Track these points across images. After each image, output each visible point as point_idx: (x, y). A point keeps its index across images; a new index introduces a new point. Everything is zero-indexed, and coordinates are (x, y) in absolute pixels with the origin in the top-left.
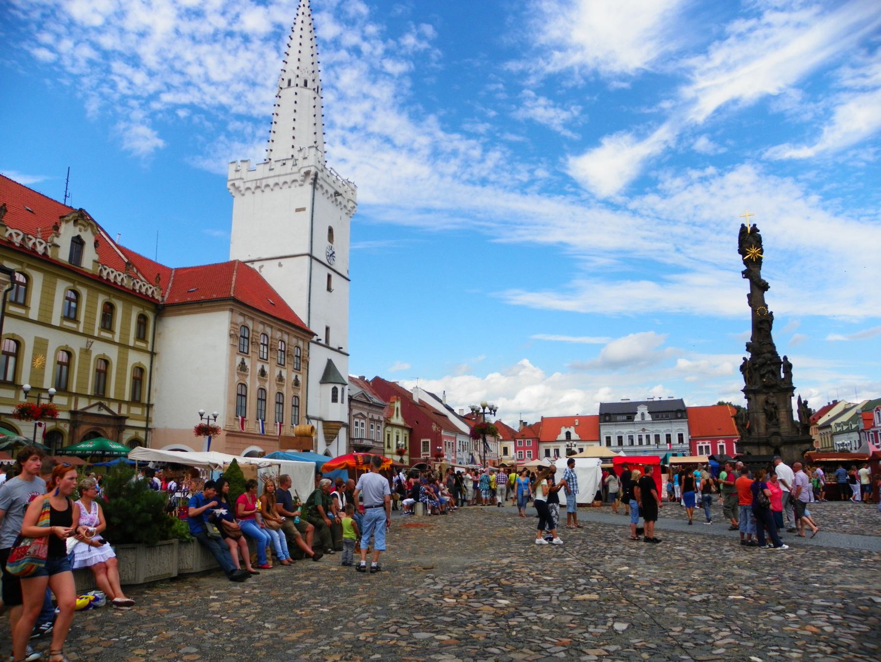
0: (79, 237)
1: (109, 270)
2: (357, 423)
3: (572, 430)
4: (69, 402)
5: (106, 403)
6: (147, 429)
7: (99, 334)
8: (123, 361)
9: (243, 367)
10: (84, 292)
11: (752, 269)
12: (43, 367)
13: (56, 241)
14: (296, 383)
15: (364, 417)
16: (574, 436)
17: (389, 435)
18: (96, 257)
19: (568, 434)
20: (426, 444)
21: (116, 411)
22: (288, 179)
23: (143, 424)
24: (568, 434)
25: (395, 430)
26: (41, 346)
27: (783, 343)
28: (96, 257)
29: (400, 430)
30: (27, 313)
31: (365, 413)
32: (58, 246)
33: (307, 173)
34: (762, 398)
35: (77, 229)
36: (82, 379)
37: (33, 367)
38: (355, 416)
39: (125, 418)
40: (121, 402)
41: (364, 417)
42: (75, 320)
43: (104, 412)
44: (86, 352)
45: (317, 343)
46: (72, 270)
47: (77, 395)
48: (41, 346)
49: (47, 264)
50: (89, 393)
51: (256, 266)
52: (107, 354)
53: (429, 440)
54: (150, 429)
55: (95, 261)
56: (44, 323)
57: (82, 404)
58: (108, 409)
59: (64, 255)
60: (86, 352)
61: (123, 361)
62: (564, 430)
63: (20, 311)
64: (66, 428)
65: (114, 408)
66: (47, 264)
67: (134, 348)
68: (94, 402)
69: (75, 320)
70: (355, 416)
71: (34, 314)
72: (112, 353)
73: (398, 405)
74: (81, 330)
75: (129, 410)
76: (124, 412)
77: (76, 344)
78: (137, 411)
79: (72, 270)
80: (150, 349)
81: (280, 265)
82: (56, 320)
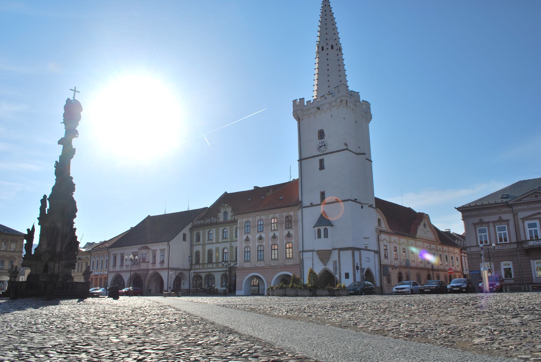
38: (524, 219)
56: (217, 242)
63: (211, 242)
69: (226, 238)
70: (524, 219)
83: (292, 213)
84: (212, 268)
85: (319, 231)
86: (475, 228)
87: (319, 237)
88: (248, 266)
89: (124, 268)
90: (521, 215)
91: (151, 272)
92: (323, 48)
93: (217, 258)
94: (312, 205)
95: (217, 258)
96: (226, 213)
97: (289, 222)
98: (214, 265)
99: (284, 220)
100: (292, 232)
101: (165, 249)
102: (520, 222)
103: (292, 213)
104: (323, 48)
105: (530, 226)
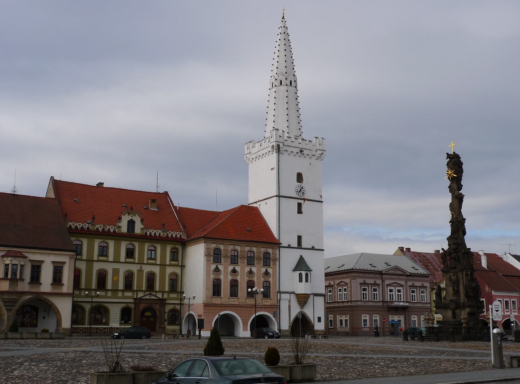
0: (132, 219)
1: (150, 231)
4: (133, 294)
5: (154, 293)
6: (181, 304)
7: (147, 261)
8: (163, 273)
9: (217, 270)
12: (118, 280)
13: (119, 224)
18: (142, 226)
21: (161, 297)
22: (267, 150)
23: (179, 302)
26: (116, 272)
28: (142, 226)
30: (108, 259)
32: (120, 227)
35: (130, 216)
36: (140, 283)
37: (113, 281)
39: (166, 300)
40: (163, 292)
43: (153, 297)
44: (140, 271)
47: (137, 291)
48: (116, 272)
50: (144, 289)
52: (153, 270)
53: (484, 300)
54: (183, 304)
55: (141, 229)
56: (117, 261)
57: (140, 295)
58: (155, 296)
59: (124, 229)
60: (140, 271)
61: (163, 273)
64: (132, 306)
65: (160, 295)
67: (170, 265)
68: (146, 293)
71: (111, 258)
72: (156, 270)
74: (136, 262)
75: (168, 296)
76: (166, 296)
77: (134, 268)
78: (174, 295)
79: (131, 236)
80: (180, 264)
81: (266, 204)
82: (123, 258)
83: (270, 251)
84: (106, 297)
86: (361, 287)
88: (218, 302)
90: (387, 282)
92: (281, 82)
93: (115, 283)
94: (289, 247)
95: (115, 283)
97: (267, 260)
98: (109, 294)
99: (262, 255)
100: (270, 270)
101: (65, 263)
102: (386, 286)
103: (270, 251)
104: (281, 82)
105: (391, 291)
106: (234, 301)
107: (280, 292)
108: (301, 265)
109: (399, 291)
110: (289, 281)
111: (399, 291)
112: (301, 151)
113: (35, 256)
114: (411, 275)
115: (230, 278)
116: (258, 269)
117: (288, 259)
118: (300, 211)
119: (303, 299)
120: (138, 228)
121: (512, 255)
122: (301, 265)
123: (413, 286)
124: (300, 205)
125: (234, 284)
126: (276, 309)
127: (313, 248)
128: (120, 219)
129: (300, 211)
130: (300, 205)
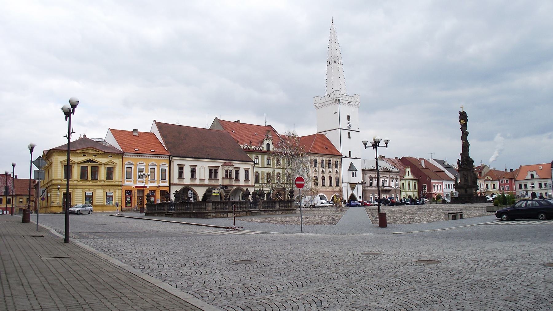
2: (383, 181)
3: (534, 173)
10: (271, 158)
11: (464, 127)
14: (337, 172)
15: (387, 178)
16: (535, 176)
17: (403, 184)
19: (532, 175)
20: (425, 186)
22: (331, 102)
24: (532, 175)
25: (407, 181)
27: (471, 154)
29: (411, 181)
31: (388, 176)
33: (336, 100)
34: (462, 172)
41: (387, 178)
42: (270, 165)
44: (274, 172)
45: (346, 157)
46: (267, 153)
48: (263, 172)
49: (262, 152)
51: (324, 133)
57: (274, 185)
59: (265, 149)
60: (274, 172)
62: (529, 173)
66: (262, 152)
69: (270, 165)
73: (409, 170)
77: (271, 171)
79: (267, 153)
83: (338, 160)
85: (353, 173)
87: (353, 176)
89: (198, 182)
91: (234, 188)
96: (268, 145)
103: (338, 160)
106: (323, 188)
107: (343, 183)
108: (352, 167)
109: (386, 181)
110: (346, 176)
111: (386, 181)
112: (349, 103)
113: (236, 165)
114: (392, 172)
115: (321, 175)
116: (333, 170)
117: (345, 163)
118: (349, 137)
119: (353, 186)
120: (271, 147)
121: (434, 160)
122: (352, 167)
123: (392, 178)
124: (349, 133)
125: (323, 178)
126: (341, 191)
127: (356, 158)
128: (263, 143)
129: (349, 137)
130: (349, 133)
